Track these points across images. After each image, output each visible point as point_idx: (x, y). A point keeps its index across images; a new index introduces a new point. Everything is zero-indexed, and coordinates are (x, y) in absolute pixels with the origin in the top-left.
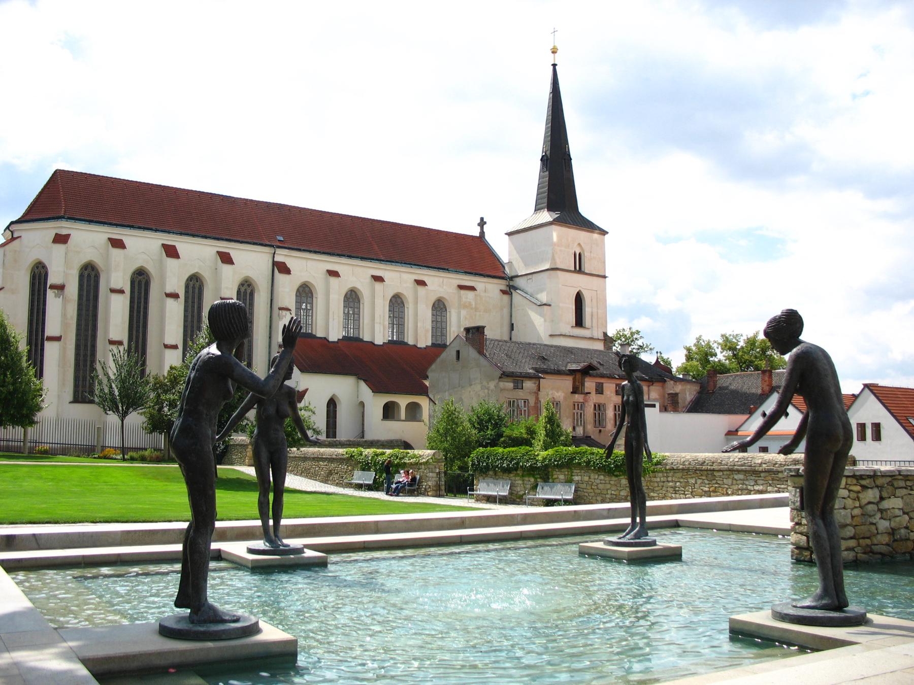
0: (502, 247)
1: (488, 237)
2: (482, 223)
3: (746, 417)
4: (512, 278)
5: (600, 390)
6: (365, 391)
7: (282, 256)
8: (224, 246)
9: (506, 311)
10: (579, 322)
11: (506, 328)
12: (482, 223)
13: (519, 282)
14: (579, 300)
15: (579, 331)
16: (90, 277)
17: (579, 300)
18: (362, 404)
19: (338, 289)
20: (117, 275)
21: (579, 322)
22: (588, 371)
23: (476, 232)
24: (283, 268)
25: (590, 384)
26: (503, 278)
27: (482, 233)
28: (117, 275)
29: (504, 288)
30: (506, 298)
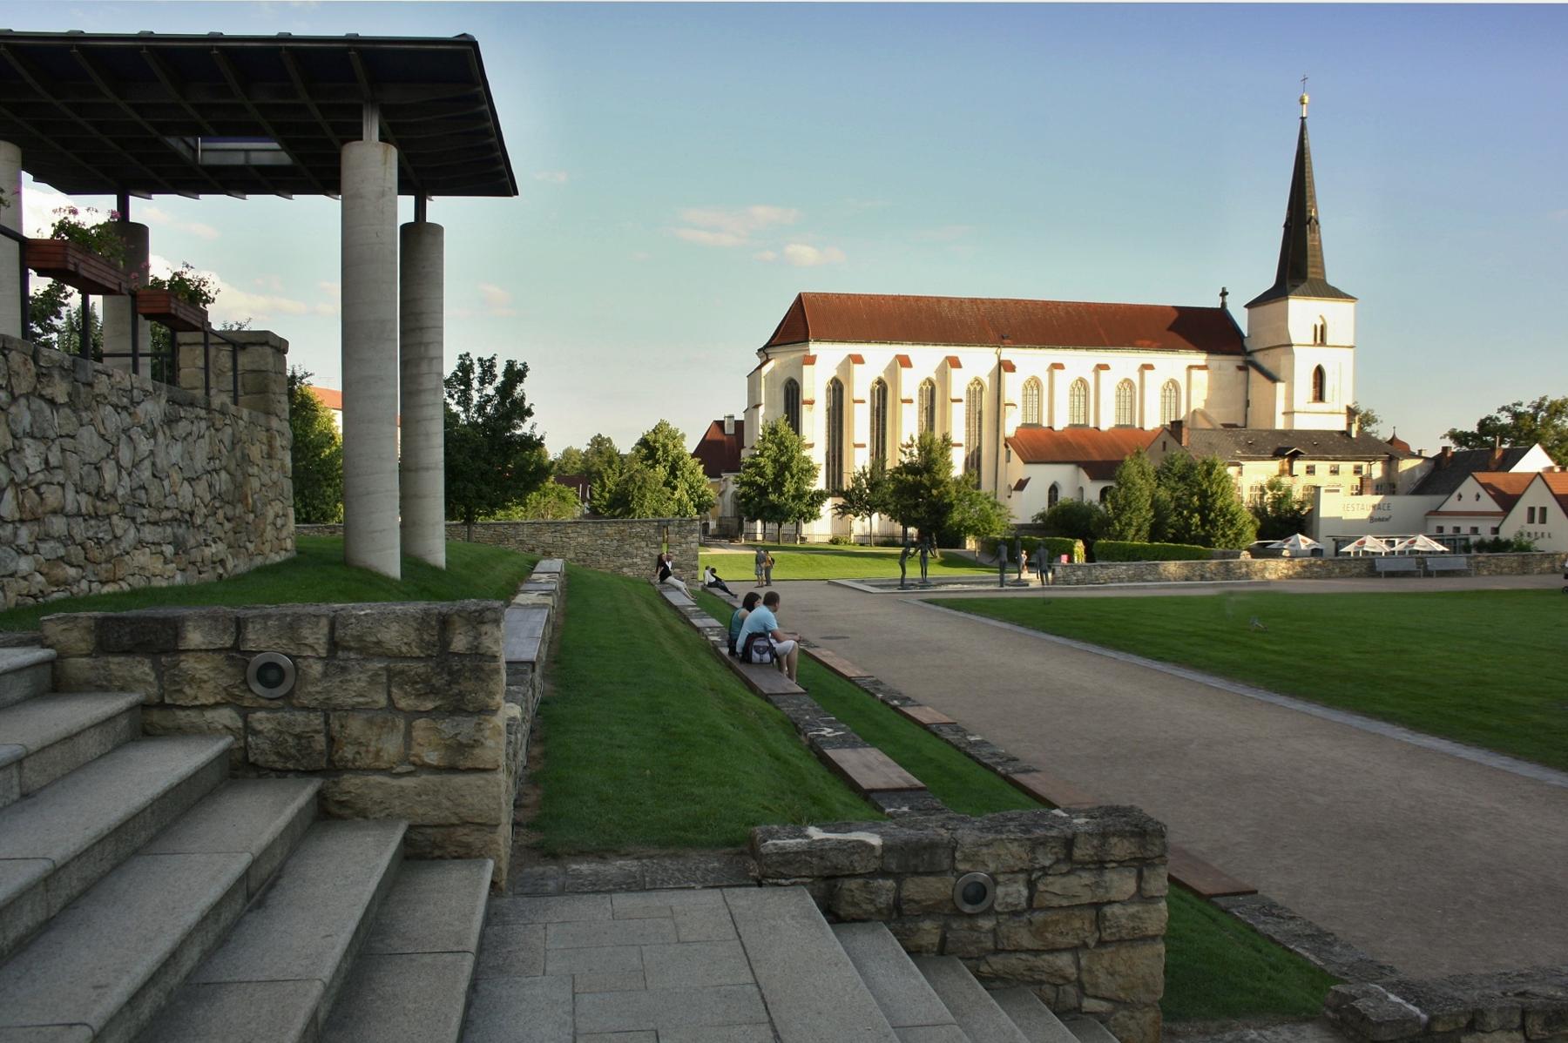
0: (1241, 318)
1: (1229, 308)
2: (1224, 294)
3: (1443, 498)
4: (1250, 353)
5: (1311, 471)
6: (1084, 478)
7: (1008, 354)
8: (952, 351)
9: (1241, 389)
10: (1320, 396)
11: (1241, 405)
12: (1224, 294)
13: (1259, 358)
14: (1319, 373)
15: (1319, 406)
16: (837, 390)
17: (1319, 373)
18: (1081, 489)
19: (1064, 381)
20: (861, 387)
21: (1320, 396)
22: (1295, 456)
23: (1216, 303)
24: (1011, 368)
25: (1299, 466)
26: (1238, 354)
27: (1224, 304)
28: (861, 387)
29: (1240, 364)
30: (1242, 374)
